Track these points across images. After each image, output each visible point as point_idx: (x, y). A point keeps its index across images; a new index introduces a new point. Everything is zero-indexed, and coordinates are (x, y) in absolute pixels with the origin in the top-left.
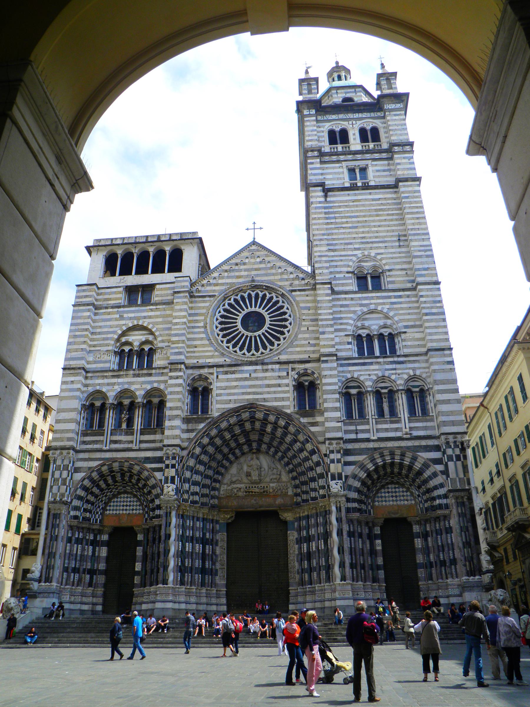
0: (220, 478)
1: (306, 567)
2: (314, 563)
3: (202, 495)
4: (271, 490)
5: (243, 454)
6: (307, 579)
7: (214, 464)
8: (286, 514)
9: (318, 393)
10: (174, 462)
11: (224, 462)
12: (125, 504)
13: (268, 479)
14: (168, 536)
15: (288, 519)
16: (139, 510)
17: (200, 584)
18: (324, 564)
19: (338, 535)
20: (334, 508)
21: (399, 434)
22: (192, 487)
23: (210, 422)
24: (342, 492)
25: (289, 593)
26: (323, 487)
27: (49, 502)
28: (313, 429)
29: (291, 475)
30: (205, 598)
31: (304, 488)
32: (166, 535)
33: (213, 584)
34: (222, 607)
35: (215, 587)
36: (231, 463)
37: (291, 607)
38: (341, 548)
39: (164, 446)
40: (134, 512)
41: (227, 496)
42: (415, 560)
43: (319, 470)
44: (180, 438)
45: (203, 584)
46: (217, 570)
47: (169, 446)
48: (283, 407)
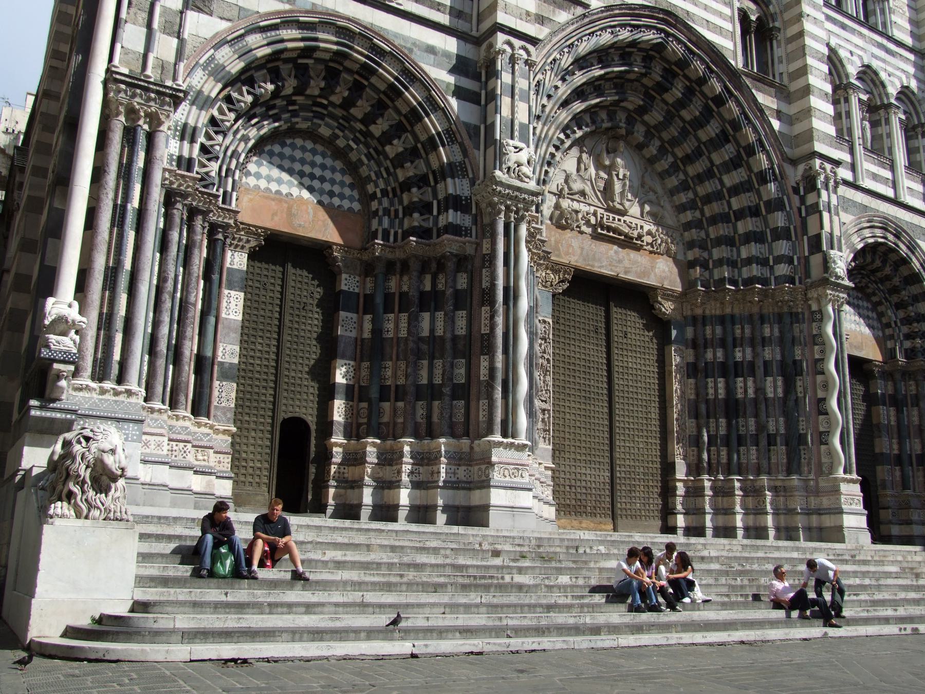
1: (722, 431)
4: (648, 239)
9: (779, 52)
12: (307, 169)
16: (351, 199)
18: (782, 431)
21: (890, 193)
27: (111, 78)
29: (689, 216)
40: (336, 201)
42: (873, 446)
43: (779, 220)
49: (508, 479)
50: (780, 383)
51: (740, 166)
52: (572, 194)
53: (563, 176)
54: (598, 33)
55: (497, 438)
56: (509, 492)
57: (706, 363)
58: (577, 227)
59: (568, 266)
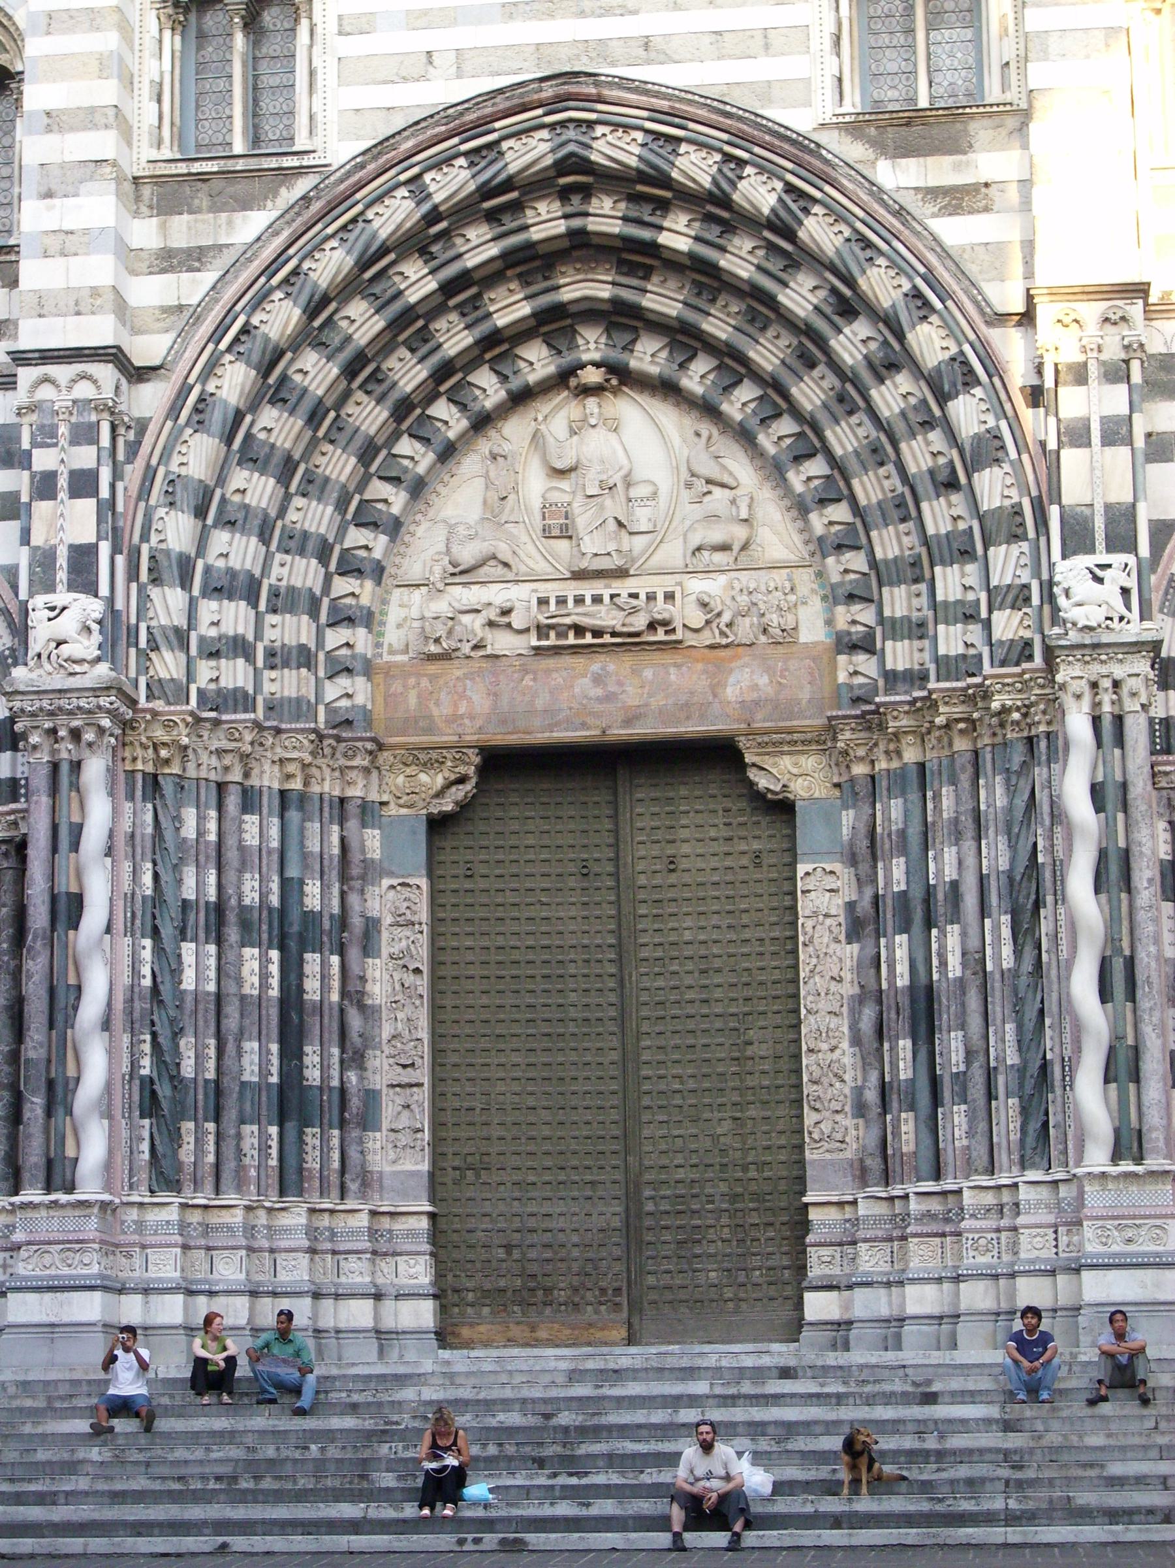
0: (379, 543)
1: (905, 1074)
2: (953, 1049)
3: (271, 654)
4: (697, 618)
5: (521, 398)
6: (908, 1147)
7: (338, 465)
8: (786, 762)
10: (85, 457)
11: (405, 446)
13: (673, 553)
14: (68, 909)
15: (799, 789)
17: (274, 1181)
18: (1012, 1058)
19: (1097, 891)
20: (1078, 725)
22: (209, 609)
23: (306, 199)
24: (1134, 630)
25: (804, 1226)
26: (1019, 597)
28: (953, 231)
29: (817, 522)
30: (304, 1260)
31: (899, 601)
32: (54, 899)
33: (351, 1177)
34: (406, 1306)
35: (363, 1196)
36: (448, 453)
37: (819, 1306)
38: (1118, 965)
39: (21, 358)
41: (431, 658)
43: (993, 487)
44: (121, 308)
45: (290, 1179)
46: (371, 1097)
47: (48, 356)
48: (766, 89)
49: (52, 1272)
50: (1006, 932)
51: (893, 367)
52: (462, 573)
53: (441, 534)
54: (370, 215)
55: (32, 1195)
56: (48, 1297)
57: (876, 897)
58: (476, 647)
59: (458, 747)
